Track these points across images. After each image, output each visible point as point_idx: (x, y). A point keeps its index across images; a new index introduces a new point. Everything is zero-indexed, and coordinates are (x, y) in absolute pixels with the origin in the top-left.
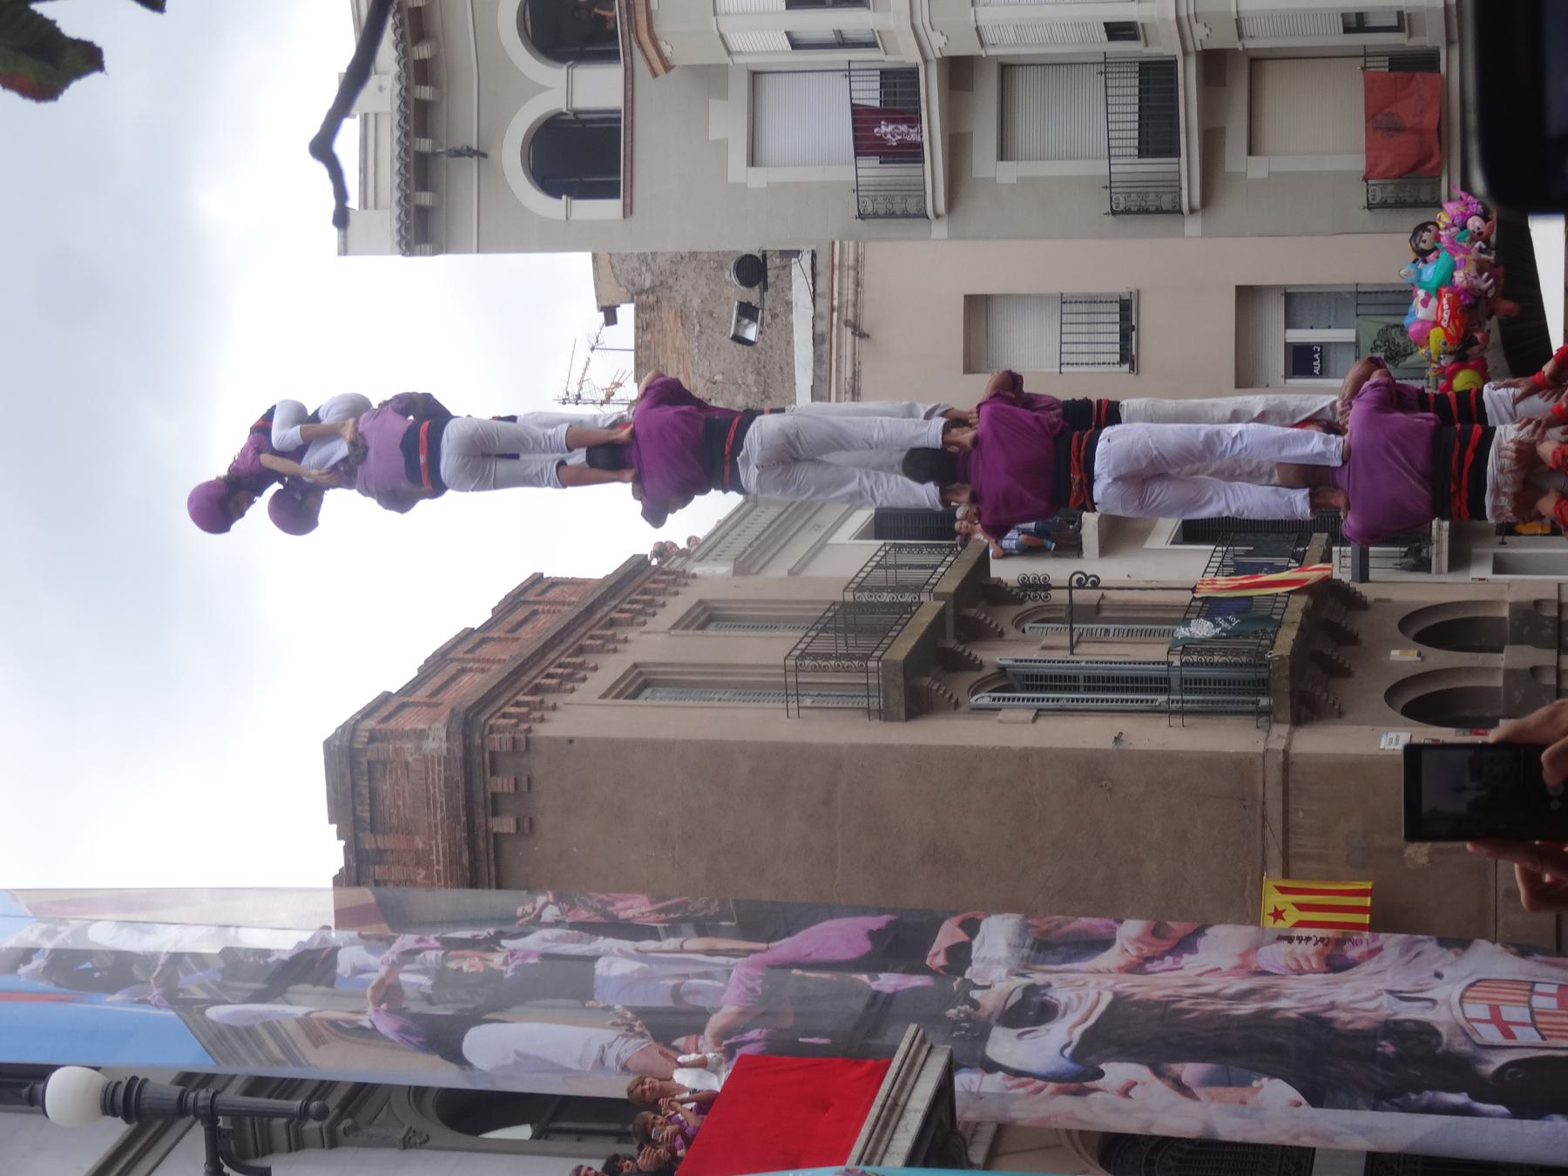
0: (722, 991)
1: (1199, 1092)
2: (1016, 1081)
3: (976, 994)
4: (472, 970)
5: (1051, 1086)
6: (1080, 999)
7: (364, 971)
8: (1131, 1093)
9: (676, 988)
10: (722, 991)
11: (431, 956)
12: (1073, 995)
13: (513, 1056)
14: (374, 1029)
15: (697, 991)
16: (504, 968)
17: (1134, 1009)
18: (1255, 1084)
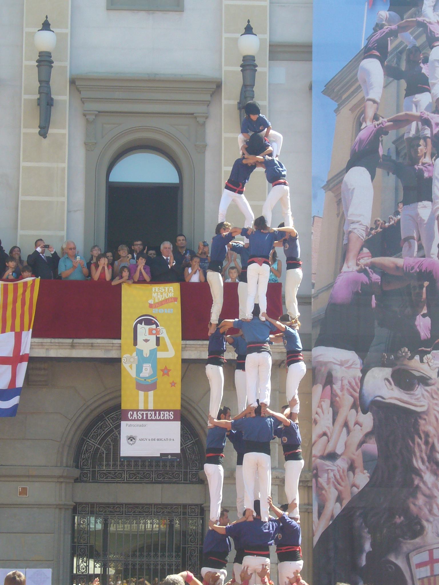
0: (411, 256)
1: (360, 451)
2: (358, 382)
3: (417, 357)
4: (419, 150)
5: (357, 395)
6: (417, 399)
7: (416, 106)
8: (357, 425)
9: (413, 238)
10: (411, 256)
11: (427, 132)
12: (419, 396)
13: (352, 188)
14: (360, 130)
15: (410, 246)
16: (420, 164)
17: (413, 420)
18: (365, 471)
